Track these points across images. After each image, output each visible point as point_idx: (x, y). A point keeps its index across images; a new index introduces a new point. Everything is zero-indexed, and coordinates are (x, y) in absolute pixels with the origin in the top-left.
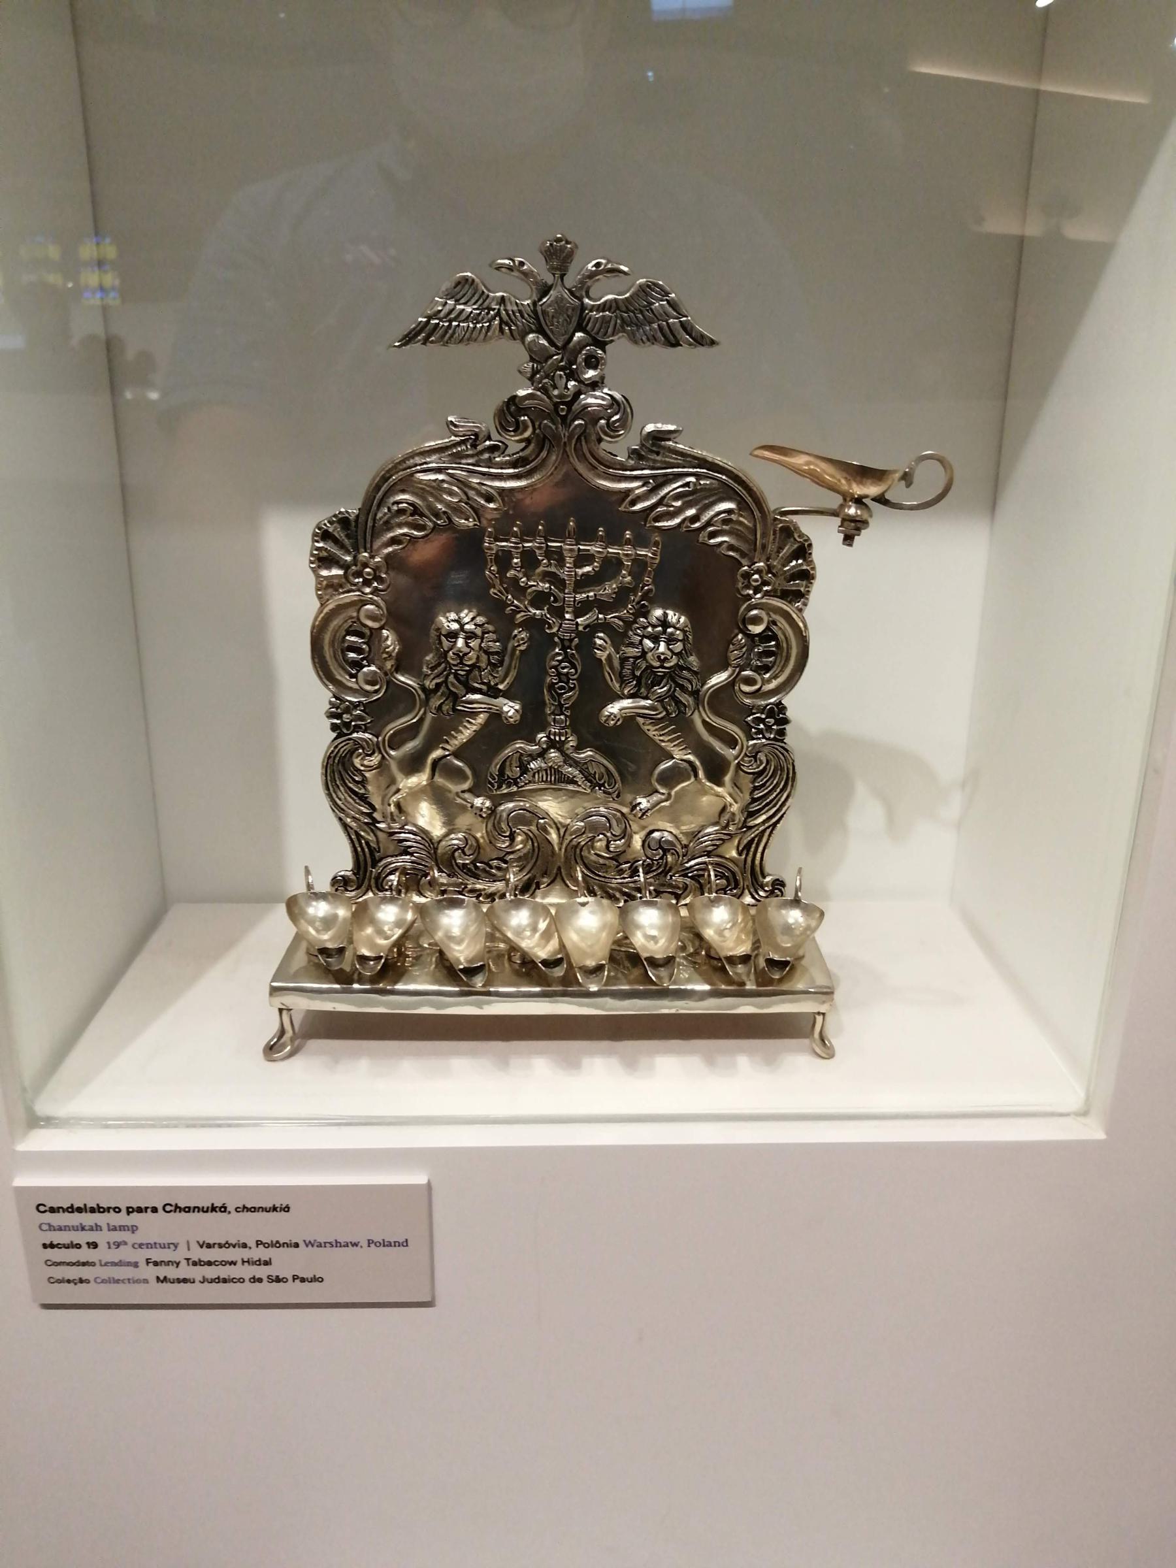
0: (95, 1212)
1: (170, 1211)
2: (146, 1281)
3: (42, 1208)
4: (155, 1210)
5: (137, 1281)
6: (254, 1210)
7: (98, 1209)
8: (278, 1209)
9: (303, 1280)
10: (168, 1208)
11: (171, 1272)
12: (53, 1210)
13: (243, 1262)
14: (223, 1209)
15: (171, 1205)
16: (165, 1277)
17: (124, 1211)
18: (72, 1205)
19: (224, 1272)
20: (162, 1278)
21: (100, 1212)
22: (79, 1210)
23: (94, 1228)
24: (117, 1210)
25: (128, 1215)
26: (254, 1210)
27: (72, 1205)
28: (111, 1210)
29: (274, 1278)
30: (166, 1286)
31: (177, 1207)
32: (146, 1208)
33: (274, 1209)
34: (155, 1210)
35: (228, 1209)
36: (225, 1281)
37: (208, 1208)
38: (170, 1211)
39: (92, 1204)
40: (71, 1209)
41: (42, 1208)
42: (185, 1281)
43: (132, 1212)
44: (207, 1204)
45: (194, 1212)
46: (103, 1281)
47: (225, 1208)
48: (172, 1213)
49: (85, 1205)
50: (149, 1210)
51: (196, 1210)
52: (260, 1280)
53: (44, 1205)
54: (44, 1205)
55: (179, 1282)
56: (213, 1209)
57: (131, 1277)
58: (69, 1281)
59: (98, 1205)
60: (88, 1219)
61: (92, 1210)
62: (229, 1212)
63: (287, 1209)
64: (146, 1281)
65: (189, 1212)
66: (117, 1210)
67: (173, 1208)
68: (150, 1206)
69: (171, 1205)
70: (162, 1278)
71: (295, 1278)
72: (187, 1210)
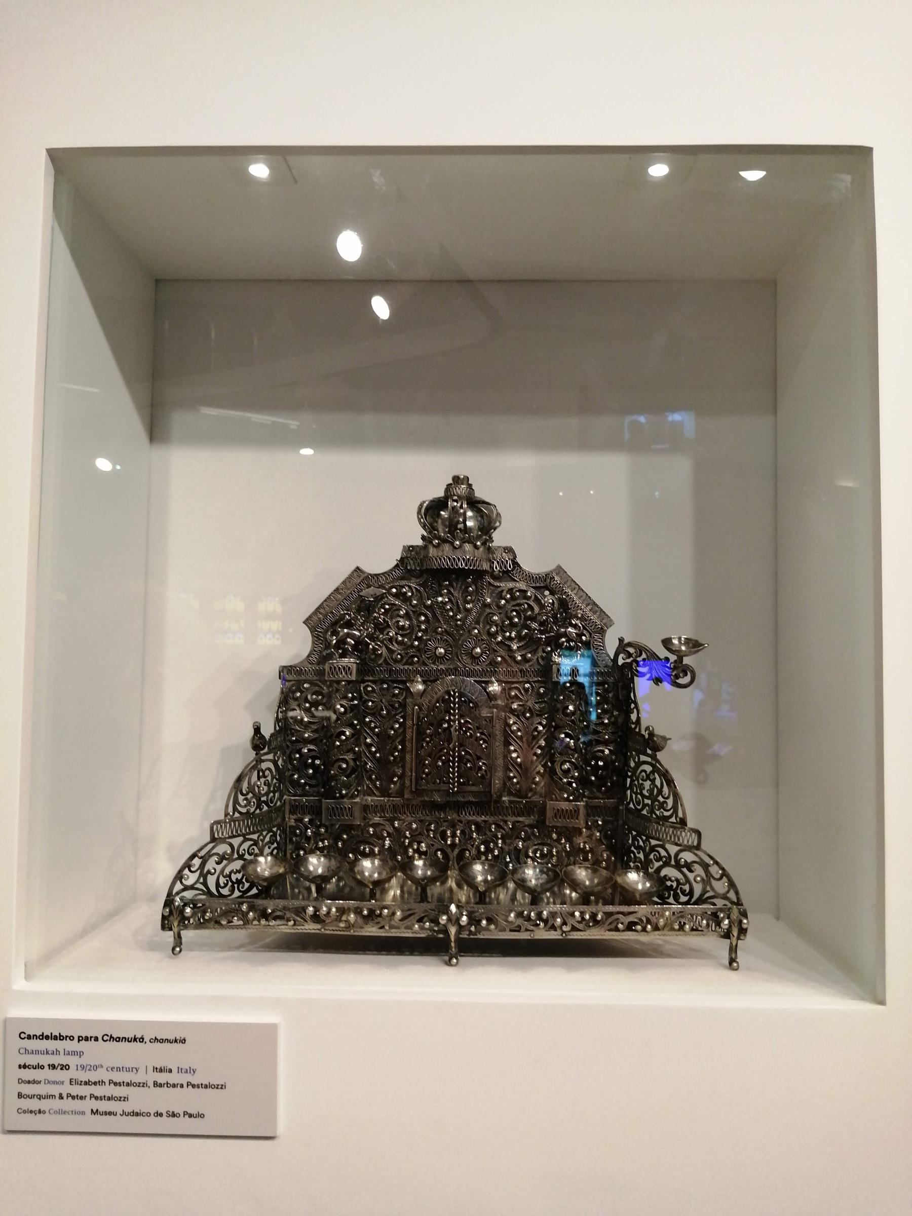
0: (57, 1039)
1: (107, 1040)
2: (83, 1113)
3: (23, 1035)
4: (96, 1039)
6: (162, 1041)
7: (61, 1038)
8: (178, 1041)
10: (106, 1038)
12: (29, 1037)
14: (142, 1040)
15: (108, 1036)
16: (97, 1110)
17: (76, 1039)
18: (43, 1033)
20: (95, 1111)
21: (60, 1039)
22: (47, 1038)
23: (55, 1053)
24: (71, 1038)
25: (79, 1042)
26: (162, 1041)
27: (43, 1033)
28: (68, 1038)
30: (97, 1117)
31: (111, 1037)
32: (91, 1037)
33: (176, 1041)
34: (96, 1039)
35: (145, 1041)
36: (137, 1114)
37: (132, 1038)
38: (107, 1040)
39: (56, 1033)
40: (43, 1037)
41: (23, 1035)
42: (110, 1113)
43: (81, 1040)
44: (130, 1035)
45: (122, 1041)
47: (143, 1039)
48: (108, 1042)
49: (51, 1034)
50: (93, 1039)
51: (124, 1040)
52: (161, 1115)
53: (25, 1033)
54: (25, 1033)
55: (106, 1115)
56: (135, 1040)
57: (74, 1110)
59: (60, 1034)
60: (51, 1045)
61: (56, 1038)
62: (146, 1042)
63: (183, 1041)
64: (83, 1113)
65: (119, 1041)
66: (71, 1038)
67: (109, 1038)
68: (94, 1036)
69: (108, 1036)
70: (95, 1111)
72: (118, 1040)
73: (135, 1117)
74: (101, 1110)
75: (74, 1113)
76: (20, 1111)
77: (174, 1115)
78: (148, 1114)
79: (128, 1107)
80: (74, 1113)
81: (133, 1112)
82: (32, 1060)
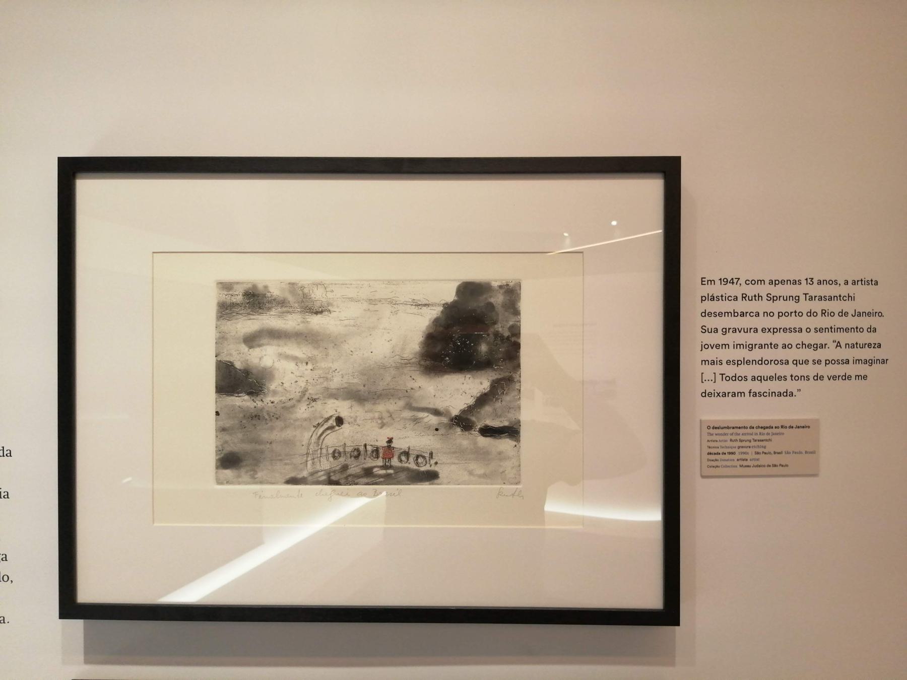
2: (736, 467)
5: (734, 466)
7: (728, 428)
9: (782, 466)
11: (745, 463)
13: (747, 460)
19: (729, 463)
42: (748, 466)
46: (724, 467)
58: (713, 467)
64: (736, 467)
71: (780, 465)
74: (744, 465)
77: (775, 466)
78: (764, 466)
79: (756, 463)
82: (714, 438)
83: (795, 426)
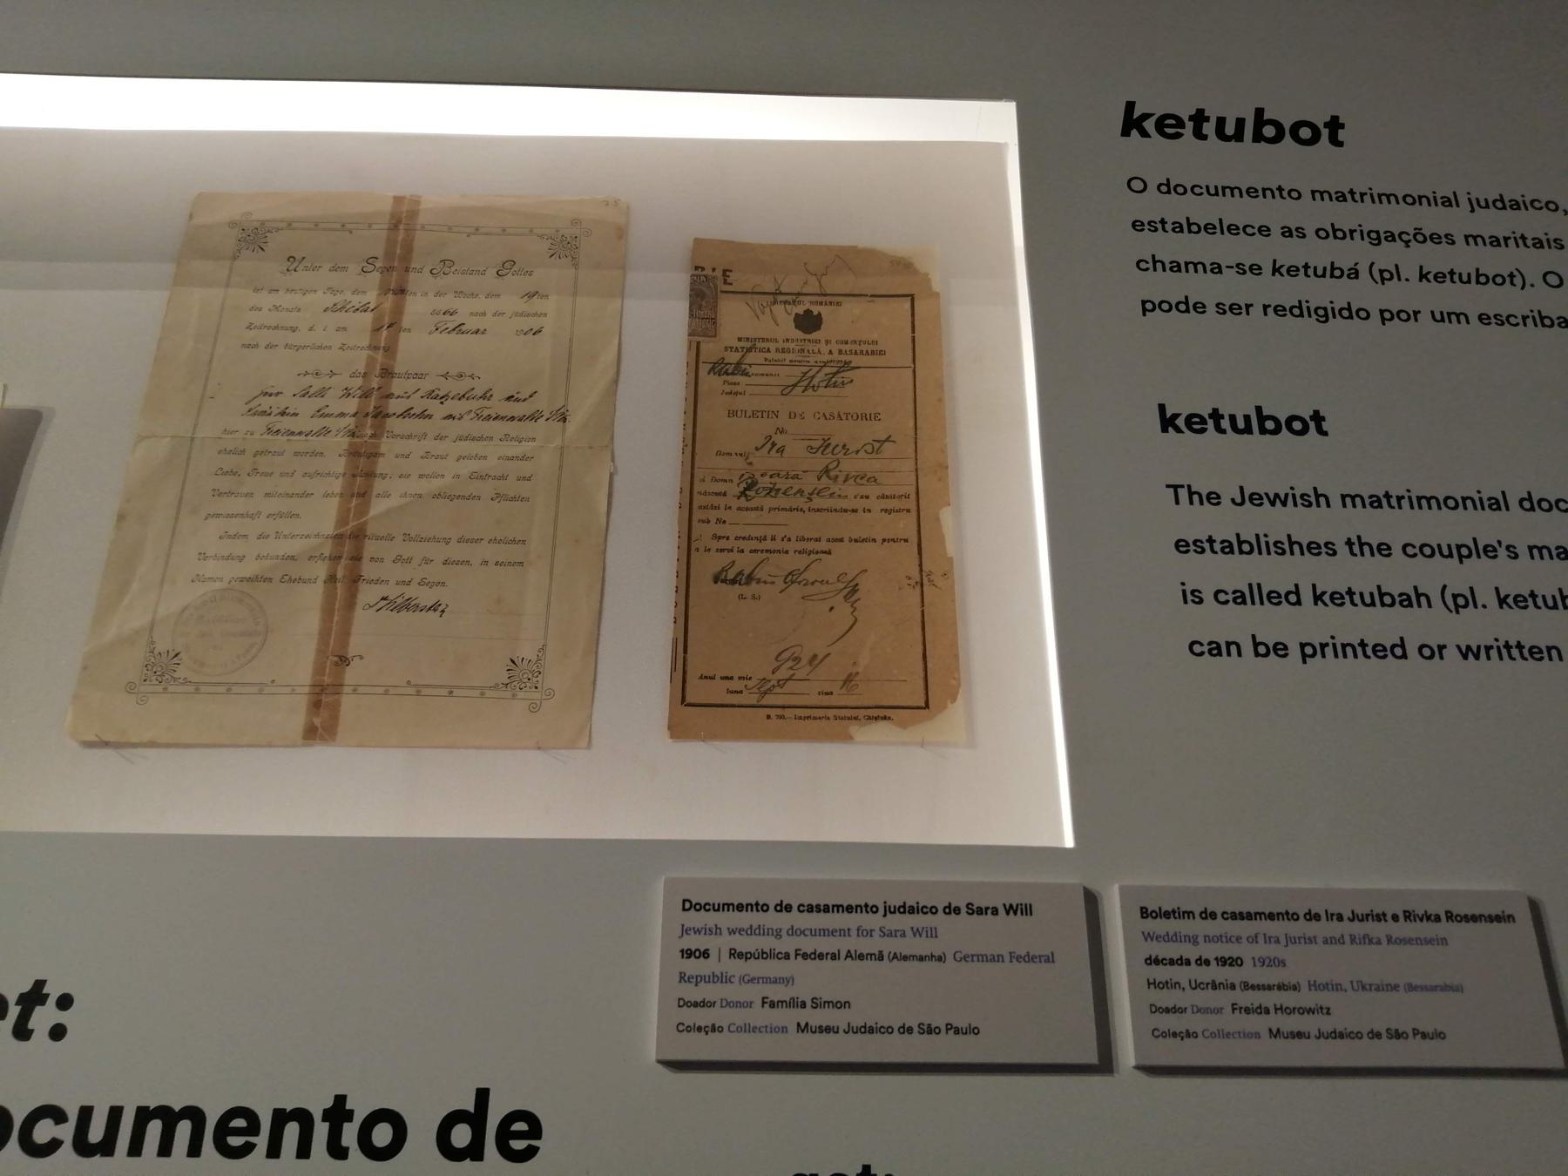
9: (957, 1031)
16: (807, 1024)
20: (803, 1025)
29: (925, 1028)
30: (808, 1036)
42: (828, 1029)
64: (784, 1030)
70: (803, 1025)
73: (867, 1035)
75: (769, 1030)
76: (681, 1028)
77: (931, 1030)
78: (889, 1030)
80: (769, 1030)
81: (865, 1027)
83: (1347, 914)
